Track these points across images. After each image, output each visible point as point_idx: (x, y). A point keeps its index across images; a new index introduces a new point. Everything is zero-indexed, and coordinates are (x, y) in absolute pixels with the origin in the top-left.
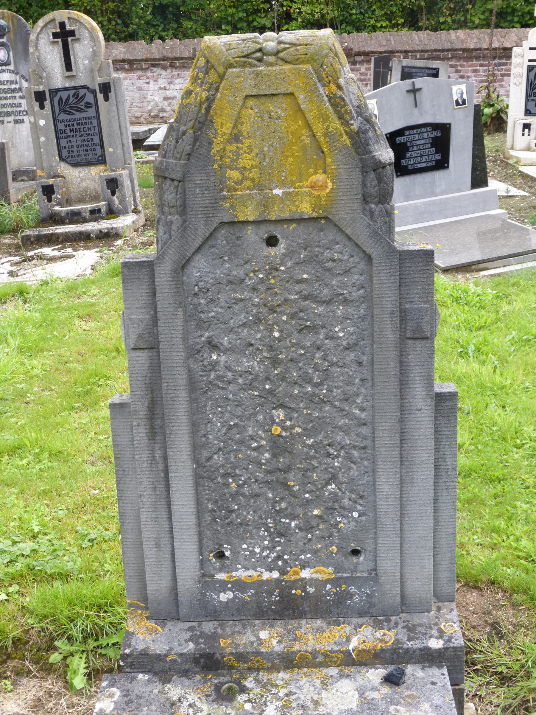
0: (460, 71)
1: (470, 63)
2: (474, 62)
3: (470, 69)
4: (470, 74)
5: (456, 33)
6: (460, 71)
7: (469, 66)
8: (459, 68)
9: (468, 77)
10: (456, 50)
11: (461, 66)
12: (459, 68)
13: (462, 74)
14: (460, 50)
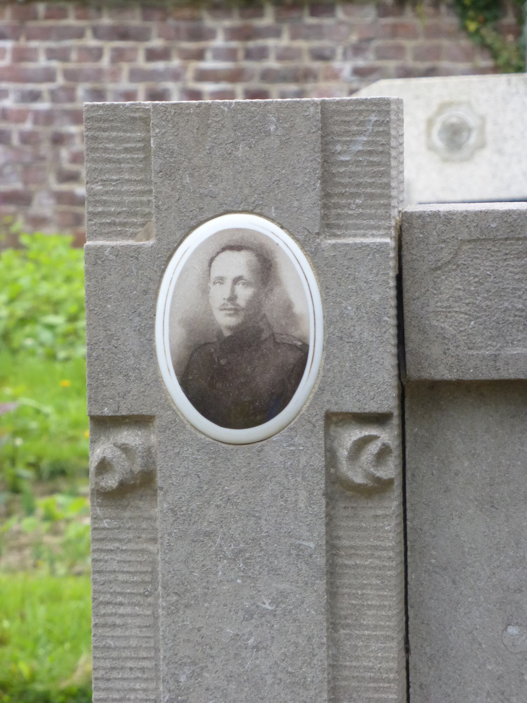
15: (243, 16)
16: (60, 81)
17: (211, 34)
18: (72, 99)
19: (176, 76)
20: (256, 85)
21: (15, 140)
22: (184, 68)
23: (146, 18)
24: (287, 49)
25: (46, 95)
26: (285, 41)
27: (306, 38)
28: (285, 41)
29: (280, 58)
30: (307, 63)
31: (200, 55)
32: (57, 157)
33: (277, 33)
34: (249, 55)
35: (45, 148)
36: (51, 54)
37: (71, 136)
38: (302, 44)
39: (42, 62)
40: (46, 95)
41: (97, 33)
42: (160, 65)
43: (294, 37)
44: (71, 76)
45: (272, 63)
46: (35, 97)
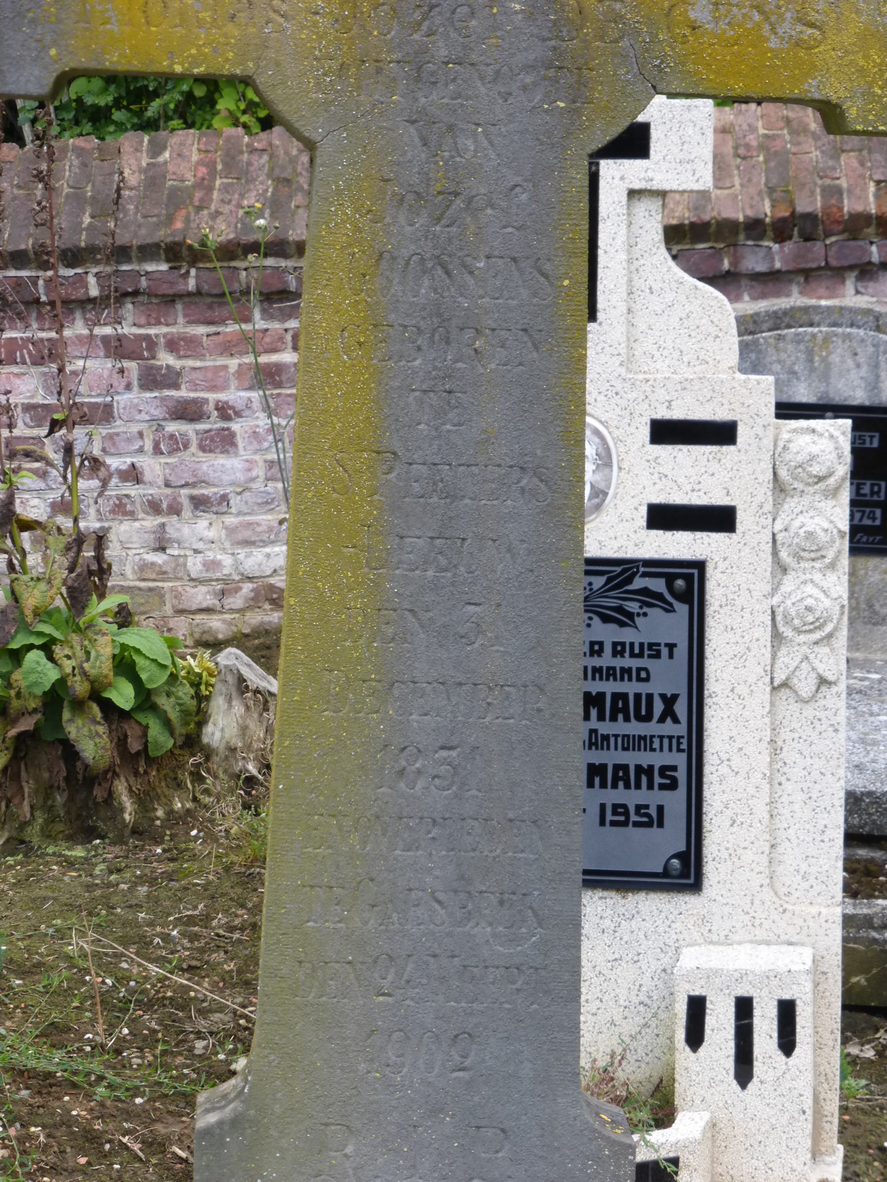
0: (171, 379)
1: (231, 328)
2: (259, 322)
3: (233, 363)
4: (235, 396)
5: (156, 149)
6: (171, 379)
7: (228, 348)
8: (165, 359)
9: (225, 412)
10: (122, 253)
11: (172, 345)
12: (165, 359)
13: (184, 393)
14: (148, 252)
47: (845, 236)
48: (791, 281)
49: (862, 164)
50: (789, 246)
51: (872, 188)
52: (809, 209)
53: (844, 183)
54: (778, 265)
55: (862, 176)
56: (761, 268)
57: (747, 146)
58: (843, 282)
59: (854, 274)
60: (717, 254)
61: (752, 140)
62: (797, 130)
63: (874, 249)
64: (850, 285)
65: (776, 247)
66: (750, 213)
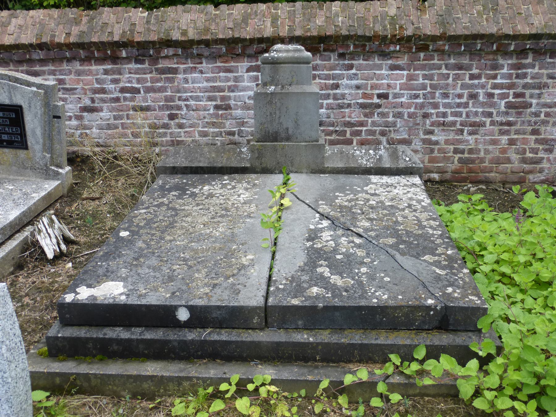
15: (517, 58)
16: (429, 89)
17: (502, 67)
18: (433, 98)
19: (483, 87)
20: (519, 90)
21: (406, 117)
22: (488, 82)
23: (471, 60)
24: (537, 73)
25: (421, 96)
26: (536, 70)
27: (547, 68)
28: (536, 70)
29: (532, 78)
30: (545, 80)
31: (495, 77)
32: (425, 124)
33: (533, 67)
34: (518, 76)
35: (419, 120)
36: (425, 77)
37: (433, 114)
38: (544, 71)
39: (421, 81)
40: (421, 96)
41: (447, 68)
42: (476, 82)
43: (540, 69)
44: (433, 87)
45: (528, 80)
46: (417, 96)
47: (58, 49)
48: (49, 62)
49: (64, 28)
50: (43, 52)
51: (64, 35)
52: (58, 41)
53: (57, 34)
54: (42, 57)
55: (62, 32)
56: (37, 58)
57: (35, 22)
58: (63, 62)
59: (65, 60)
60: (25, 54)
61: (37, 20)
62: (51, 17)
63: (67, 53)
64: (65, 64)
65: (40, 52)
66: (29, 42)
